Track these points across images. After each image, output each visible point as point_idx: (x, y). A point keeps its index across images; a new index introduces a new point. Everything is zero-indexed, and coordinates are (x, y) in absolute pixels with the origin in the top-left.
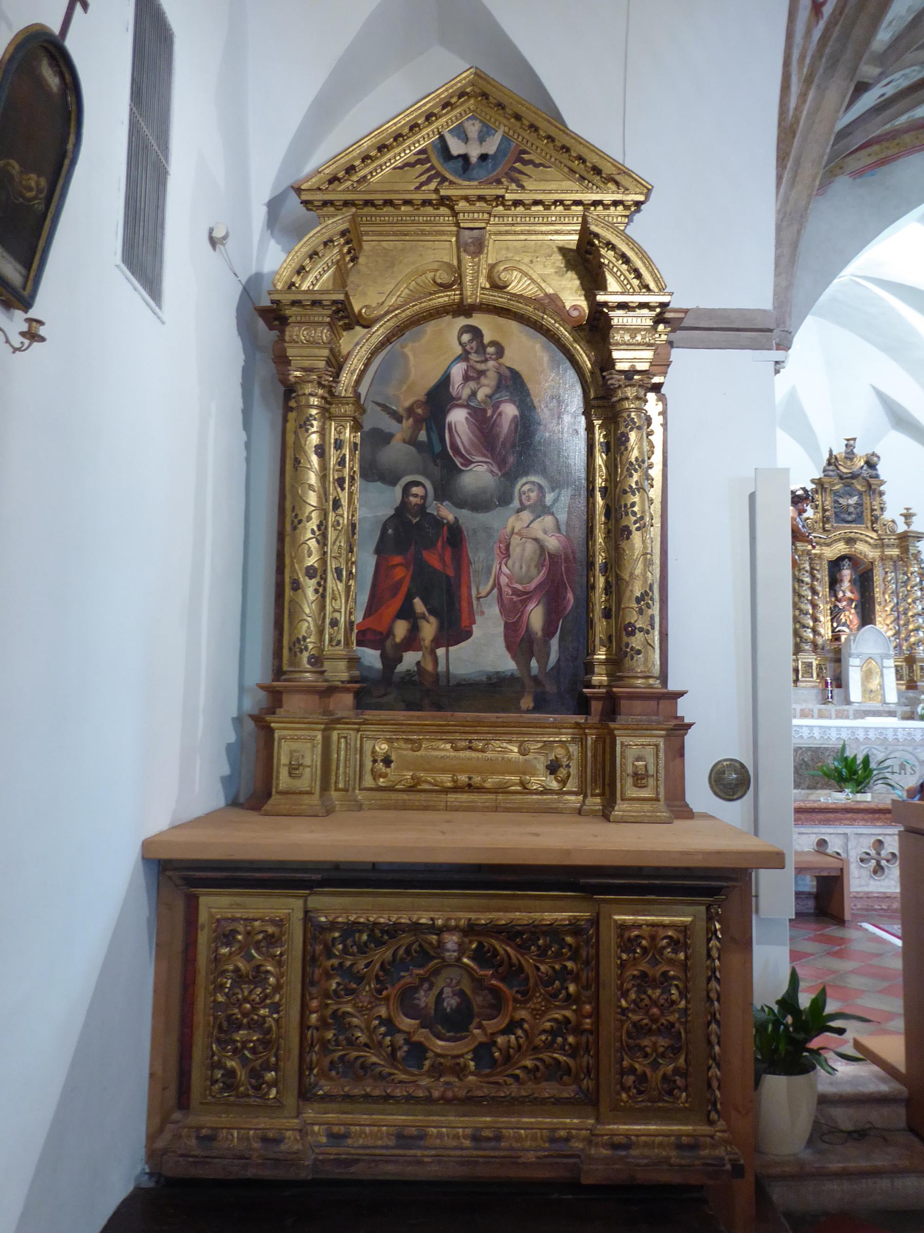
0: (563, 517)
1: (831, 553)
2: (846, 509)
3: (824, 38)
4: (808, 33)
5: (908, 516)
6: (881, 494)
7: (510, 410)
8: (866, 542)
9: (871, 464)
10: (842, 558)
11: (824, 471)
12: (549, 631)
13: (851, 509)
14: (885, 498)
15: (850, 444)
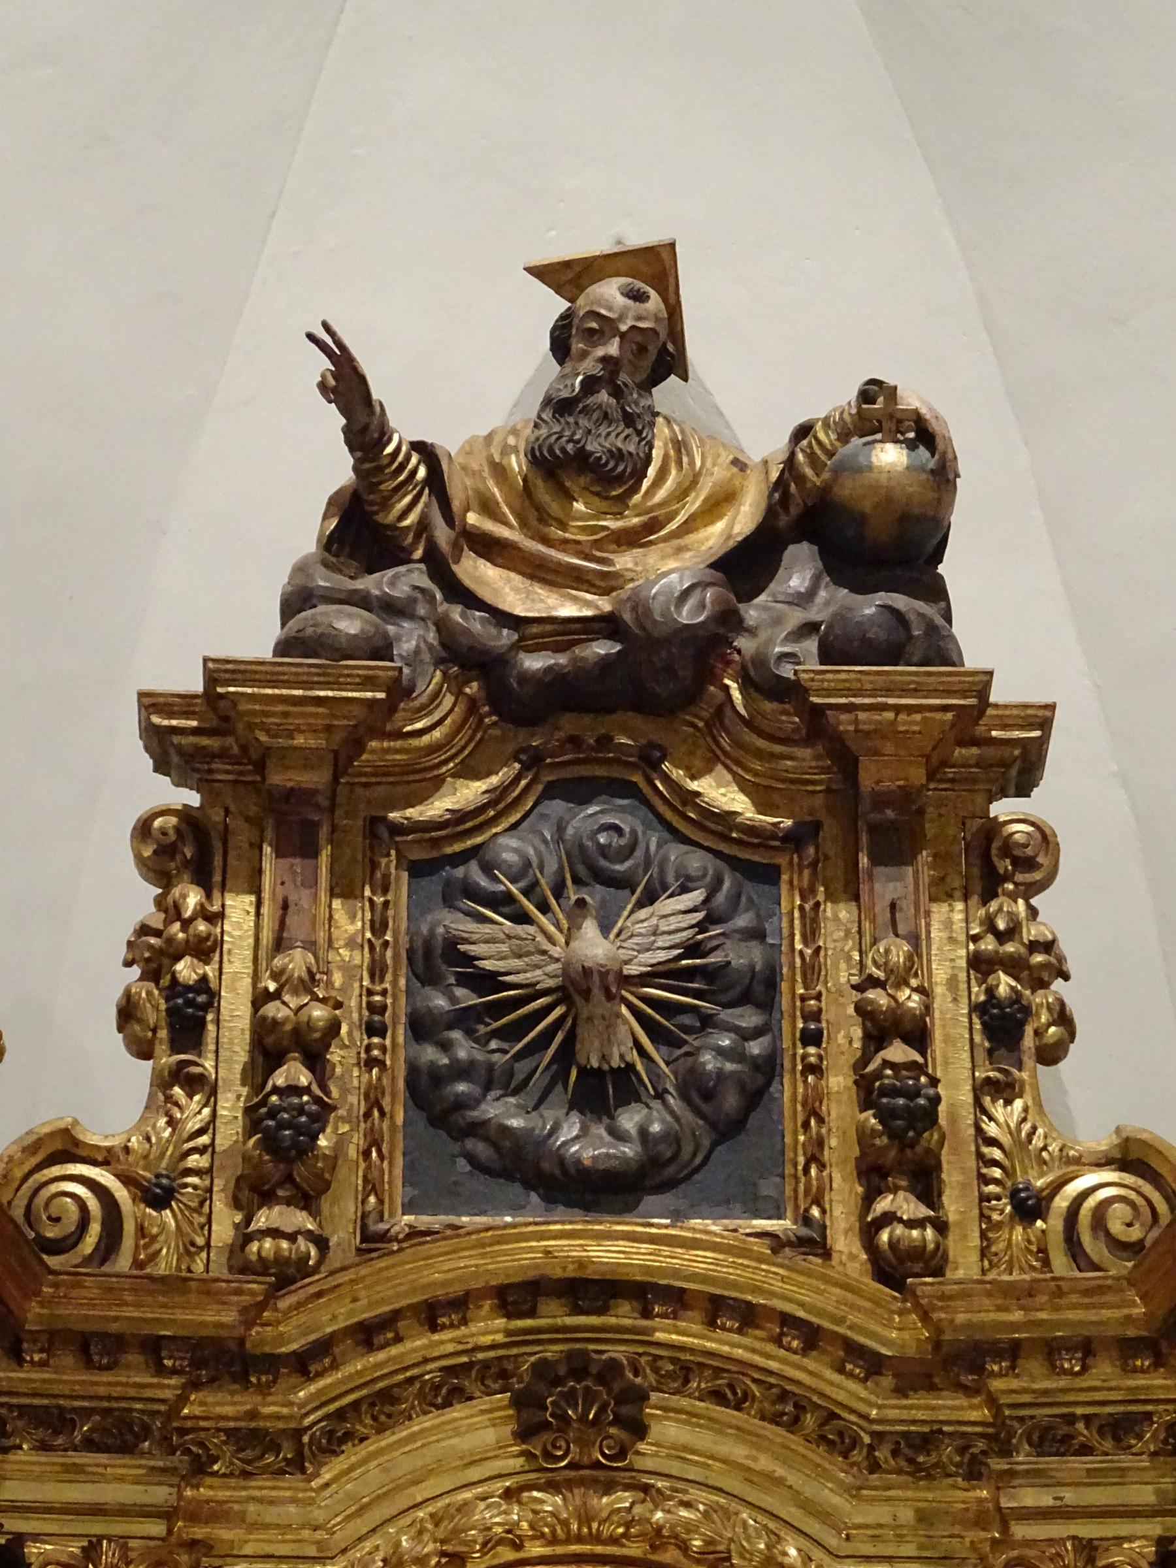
2: (551, 1031)
6: (1003, 867)
8: (788, 1408)
9: (865, 522)
11: (296, 602)
13: (621, 1039)
14: (1056, 912)
15: (620, 340)
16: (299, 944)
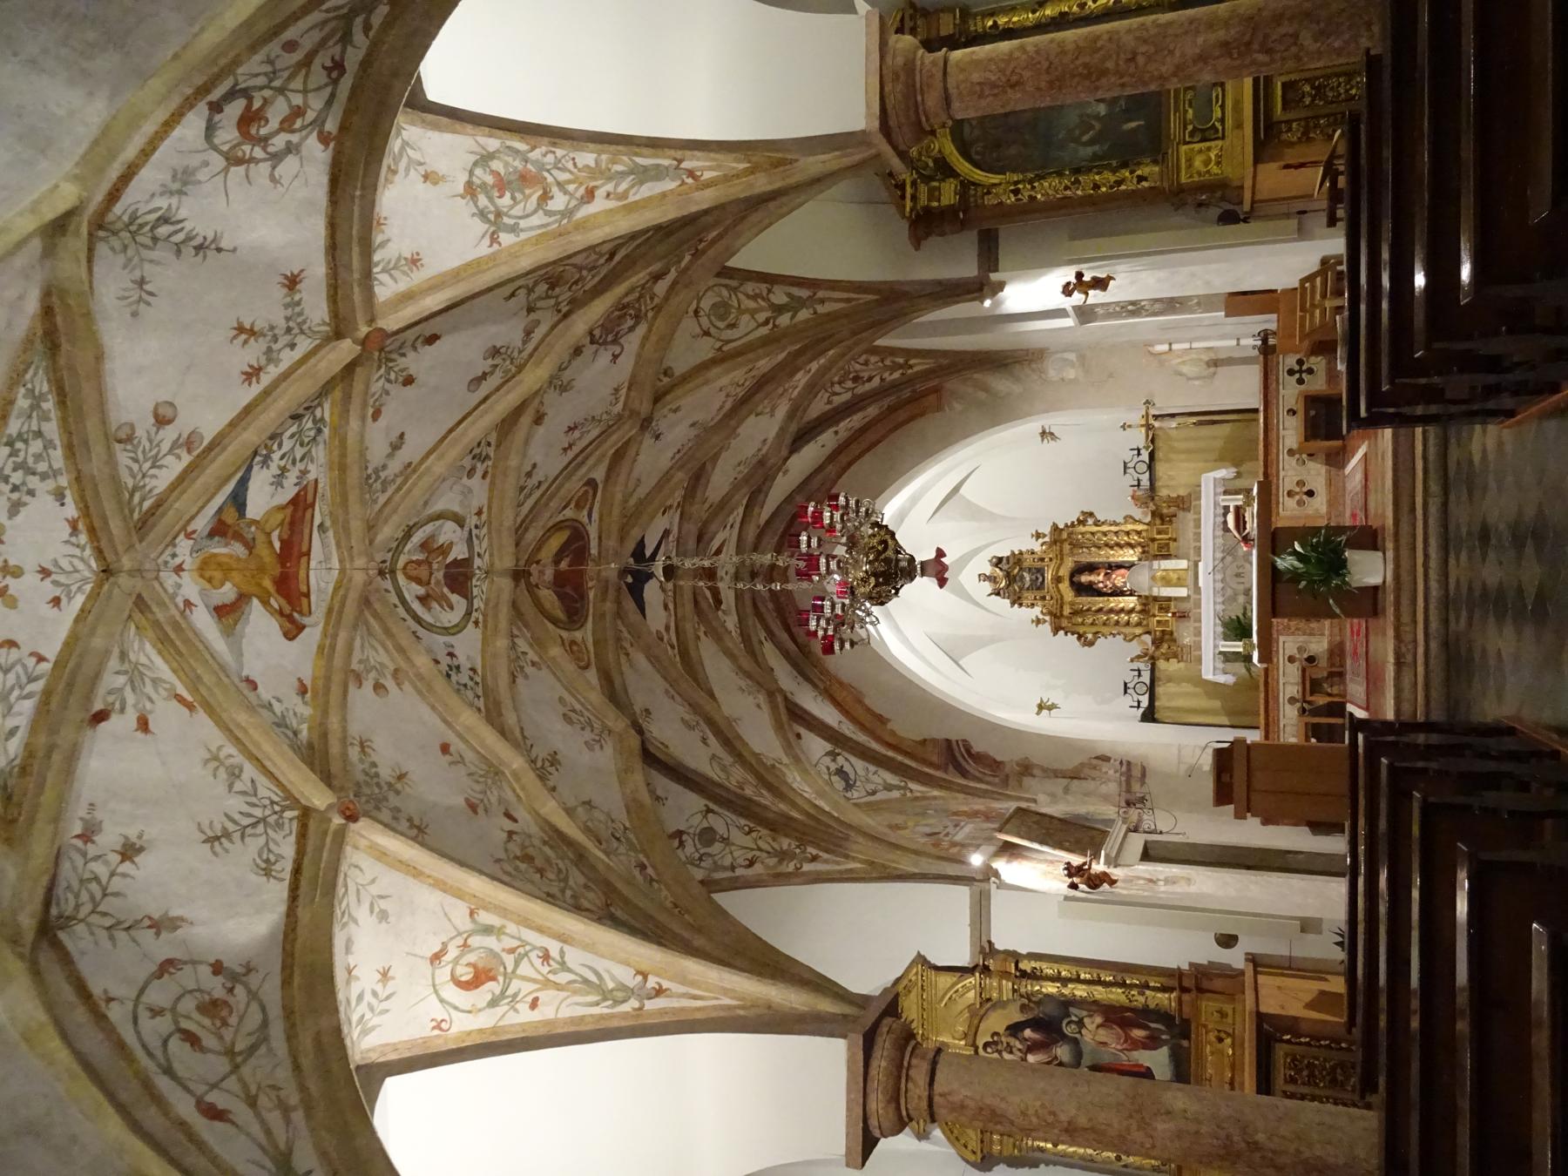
0: (1085, 1013)
1: (1068, 593)
2: (1033, 581)
3: (827, 851)
4: (826, 861)
5: (1038, 536)
6: (1021, 553)
7: (1028, 1033)
9: (998, 562)
10: (1072, 583)
12: (1145, 1027)
15: (983, 577)
16: (1029, 596)
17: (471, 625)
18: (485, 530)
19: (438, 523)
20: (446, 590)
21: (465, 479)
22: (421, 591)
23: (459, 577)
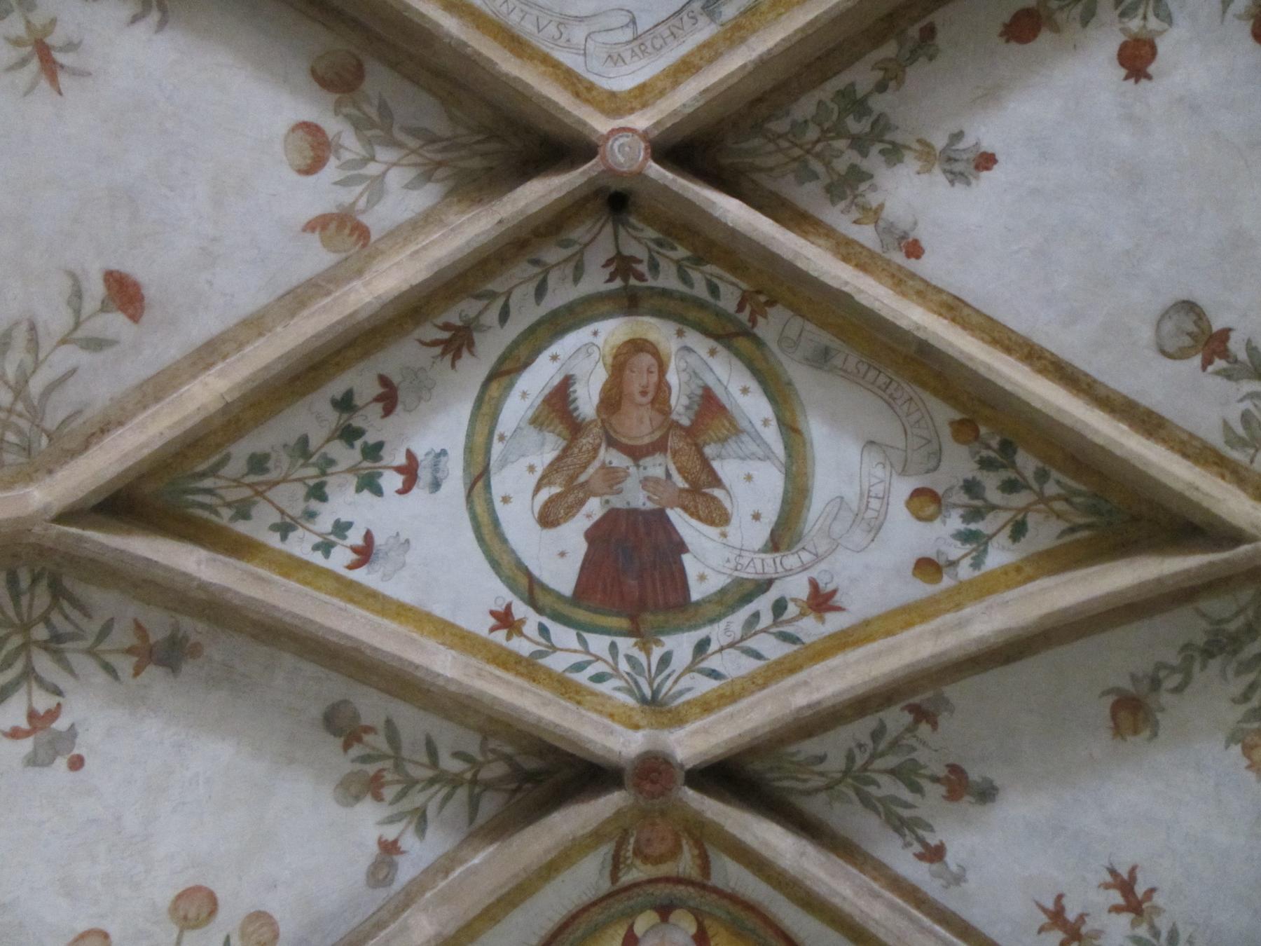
17: (497, 593)
18: (773, 649)
19: (772, 435)
20: (594, 508)
21: (903, 488)
22: (587, 400)
23: (633, 576)
